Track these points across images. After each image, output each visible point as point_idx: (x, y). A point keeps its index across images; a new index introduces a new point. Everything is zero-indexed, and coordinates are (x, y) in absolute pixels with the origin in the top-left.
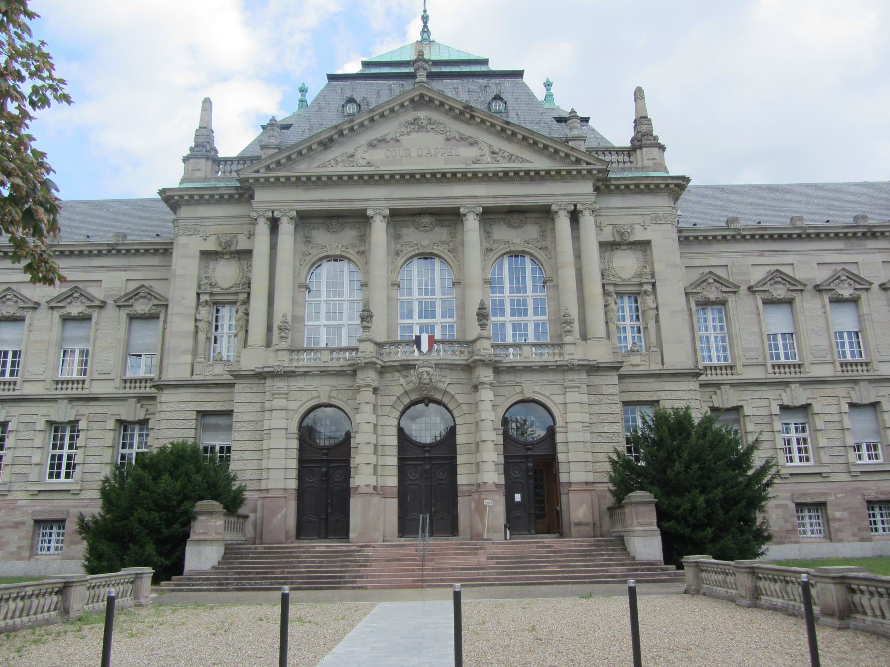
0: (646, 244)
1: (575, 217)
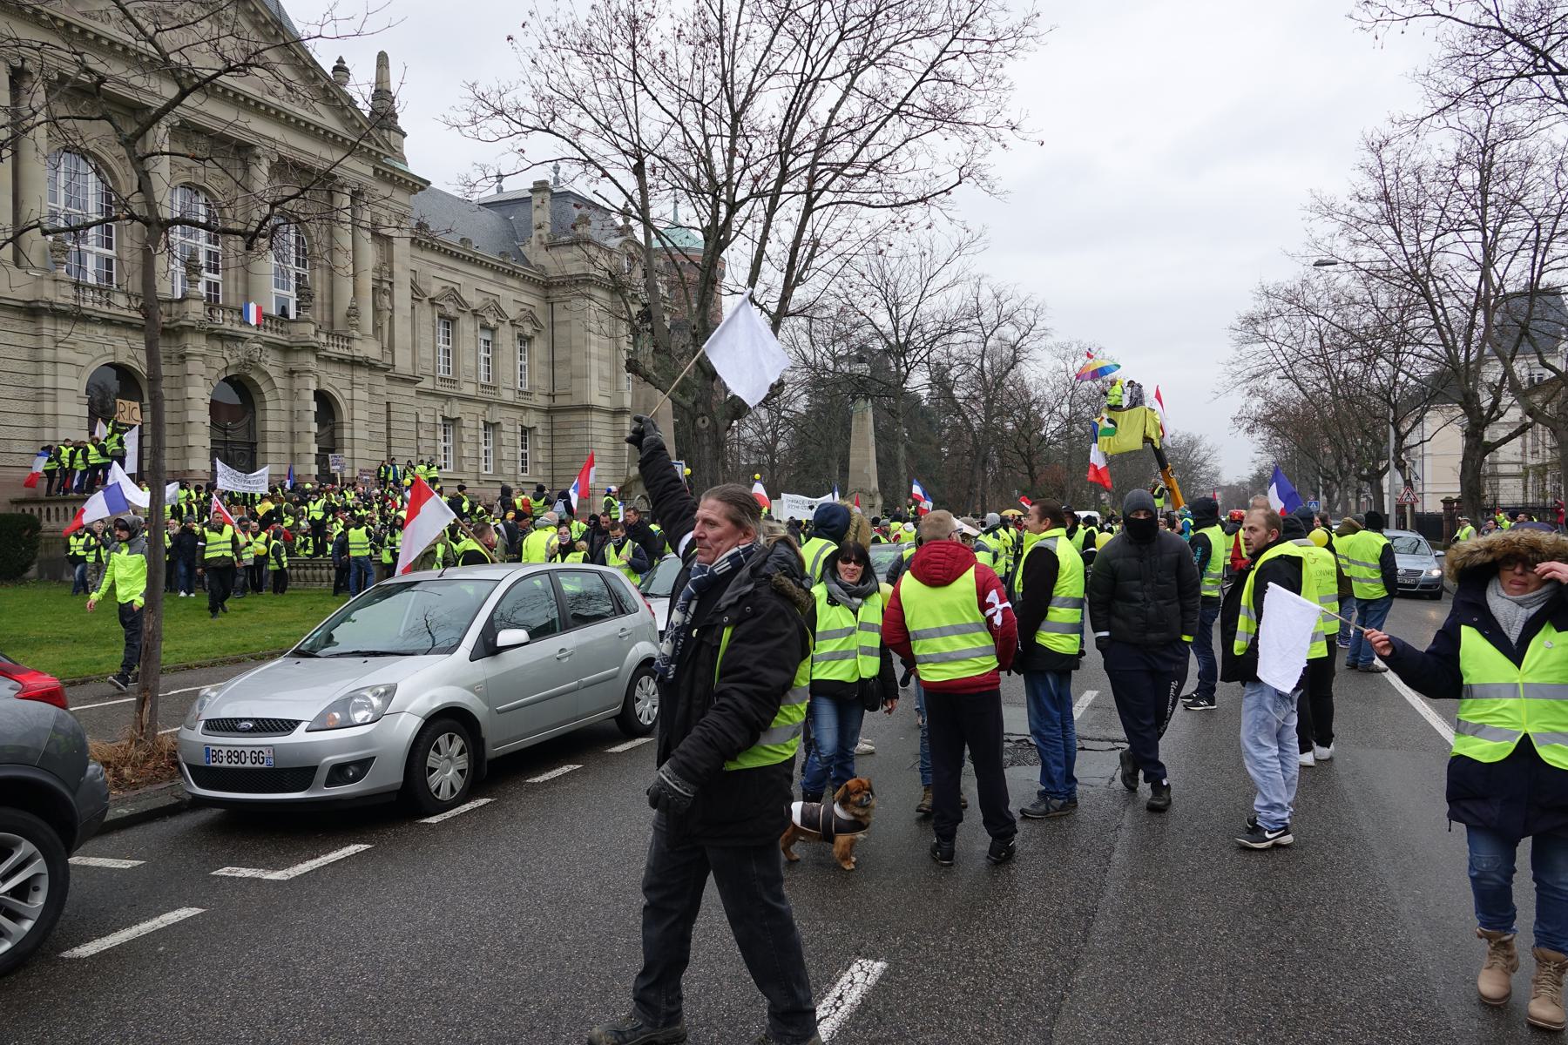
0: (389, 238)
1: (356, 195)
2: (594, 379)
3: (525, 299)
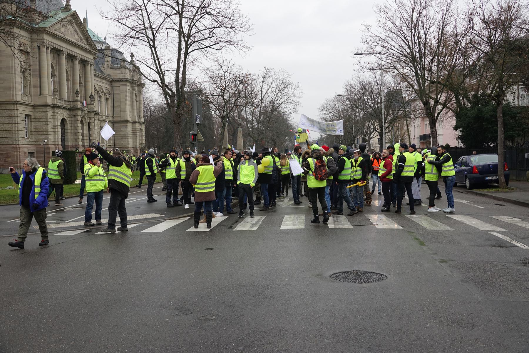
2: (128, 111)
3: (107, 86)
